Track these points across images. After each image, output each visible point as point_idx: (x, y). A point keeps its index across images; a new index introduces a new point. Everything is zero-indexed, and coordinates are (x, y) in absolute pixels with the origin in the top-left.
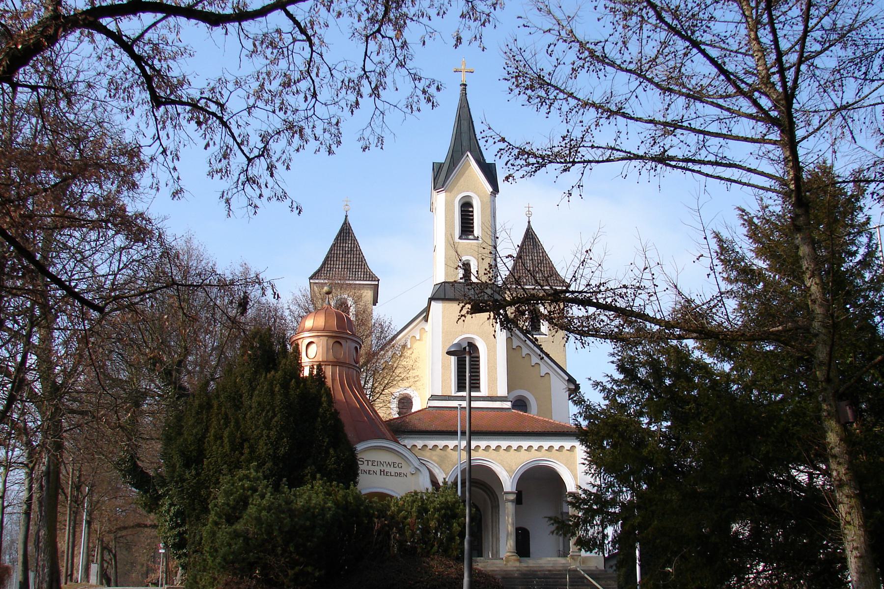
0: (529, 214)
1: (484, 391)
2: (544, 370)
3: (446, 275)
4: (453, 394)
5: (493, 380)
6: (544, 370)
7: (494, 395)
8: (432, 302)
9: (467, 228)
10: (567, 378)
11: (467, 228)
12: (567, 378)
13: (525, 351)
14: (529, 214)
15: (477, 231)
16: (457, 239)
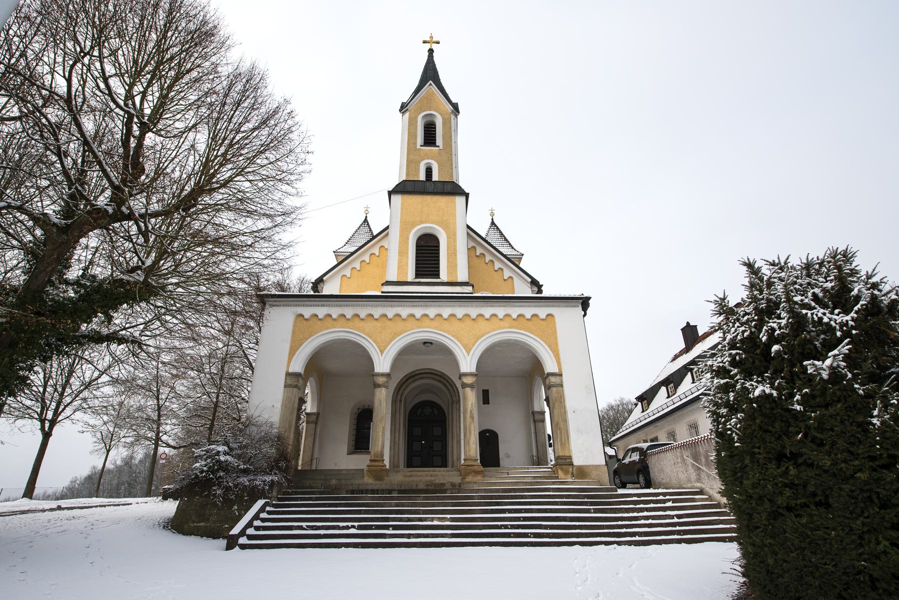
0: (492, 215)
1: (444, 276)
2: (507, 274)
3: (407, 174)
4: (409, 280)
5: (453, 266)
6: (507, 274)
7: (454, 280)
8: (392, 196)
9: (430, 138)
10: (530, 280)
11: (430, 138)
12: (530, 280)
13: (488, 258)
14: (492, 215)
15: (439, 141)
16: (419, 147)
